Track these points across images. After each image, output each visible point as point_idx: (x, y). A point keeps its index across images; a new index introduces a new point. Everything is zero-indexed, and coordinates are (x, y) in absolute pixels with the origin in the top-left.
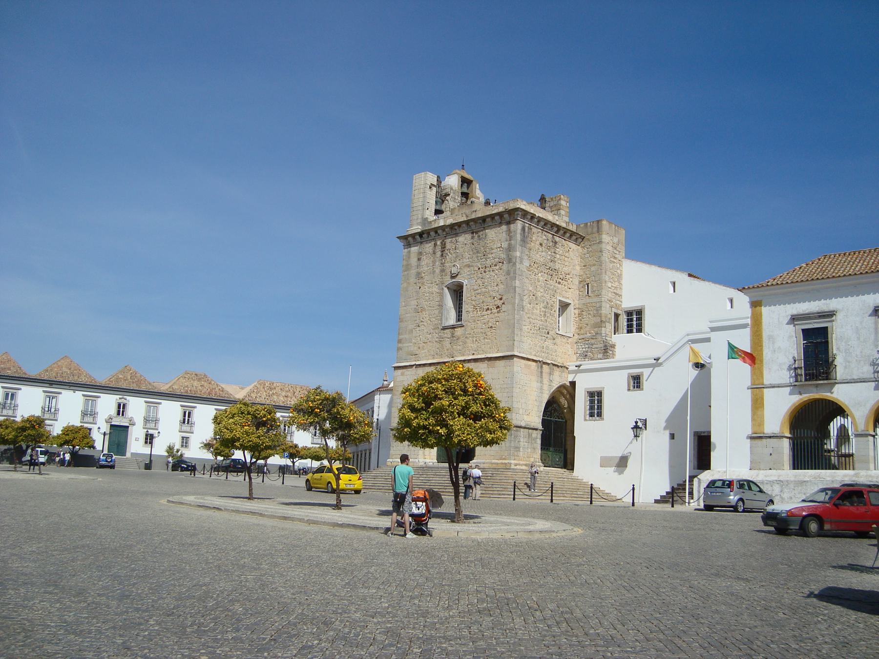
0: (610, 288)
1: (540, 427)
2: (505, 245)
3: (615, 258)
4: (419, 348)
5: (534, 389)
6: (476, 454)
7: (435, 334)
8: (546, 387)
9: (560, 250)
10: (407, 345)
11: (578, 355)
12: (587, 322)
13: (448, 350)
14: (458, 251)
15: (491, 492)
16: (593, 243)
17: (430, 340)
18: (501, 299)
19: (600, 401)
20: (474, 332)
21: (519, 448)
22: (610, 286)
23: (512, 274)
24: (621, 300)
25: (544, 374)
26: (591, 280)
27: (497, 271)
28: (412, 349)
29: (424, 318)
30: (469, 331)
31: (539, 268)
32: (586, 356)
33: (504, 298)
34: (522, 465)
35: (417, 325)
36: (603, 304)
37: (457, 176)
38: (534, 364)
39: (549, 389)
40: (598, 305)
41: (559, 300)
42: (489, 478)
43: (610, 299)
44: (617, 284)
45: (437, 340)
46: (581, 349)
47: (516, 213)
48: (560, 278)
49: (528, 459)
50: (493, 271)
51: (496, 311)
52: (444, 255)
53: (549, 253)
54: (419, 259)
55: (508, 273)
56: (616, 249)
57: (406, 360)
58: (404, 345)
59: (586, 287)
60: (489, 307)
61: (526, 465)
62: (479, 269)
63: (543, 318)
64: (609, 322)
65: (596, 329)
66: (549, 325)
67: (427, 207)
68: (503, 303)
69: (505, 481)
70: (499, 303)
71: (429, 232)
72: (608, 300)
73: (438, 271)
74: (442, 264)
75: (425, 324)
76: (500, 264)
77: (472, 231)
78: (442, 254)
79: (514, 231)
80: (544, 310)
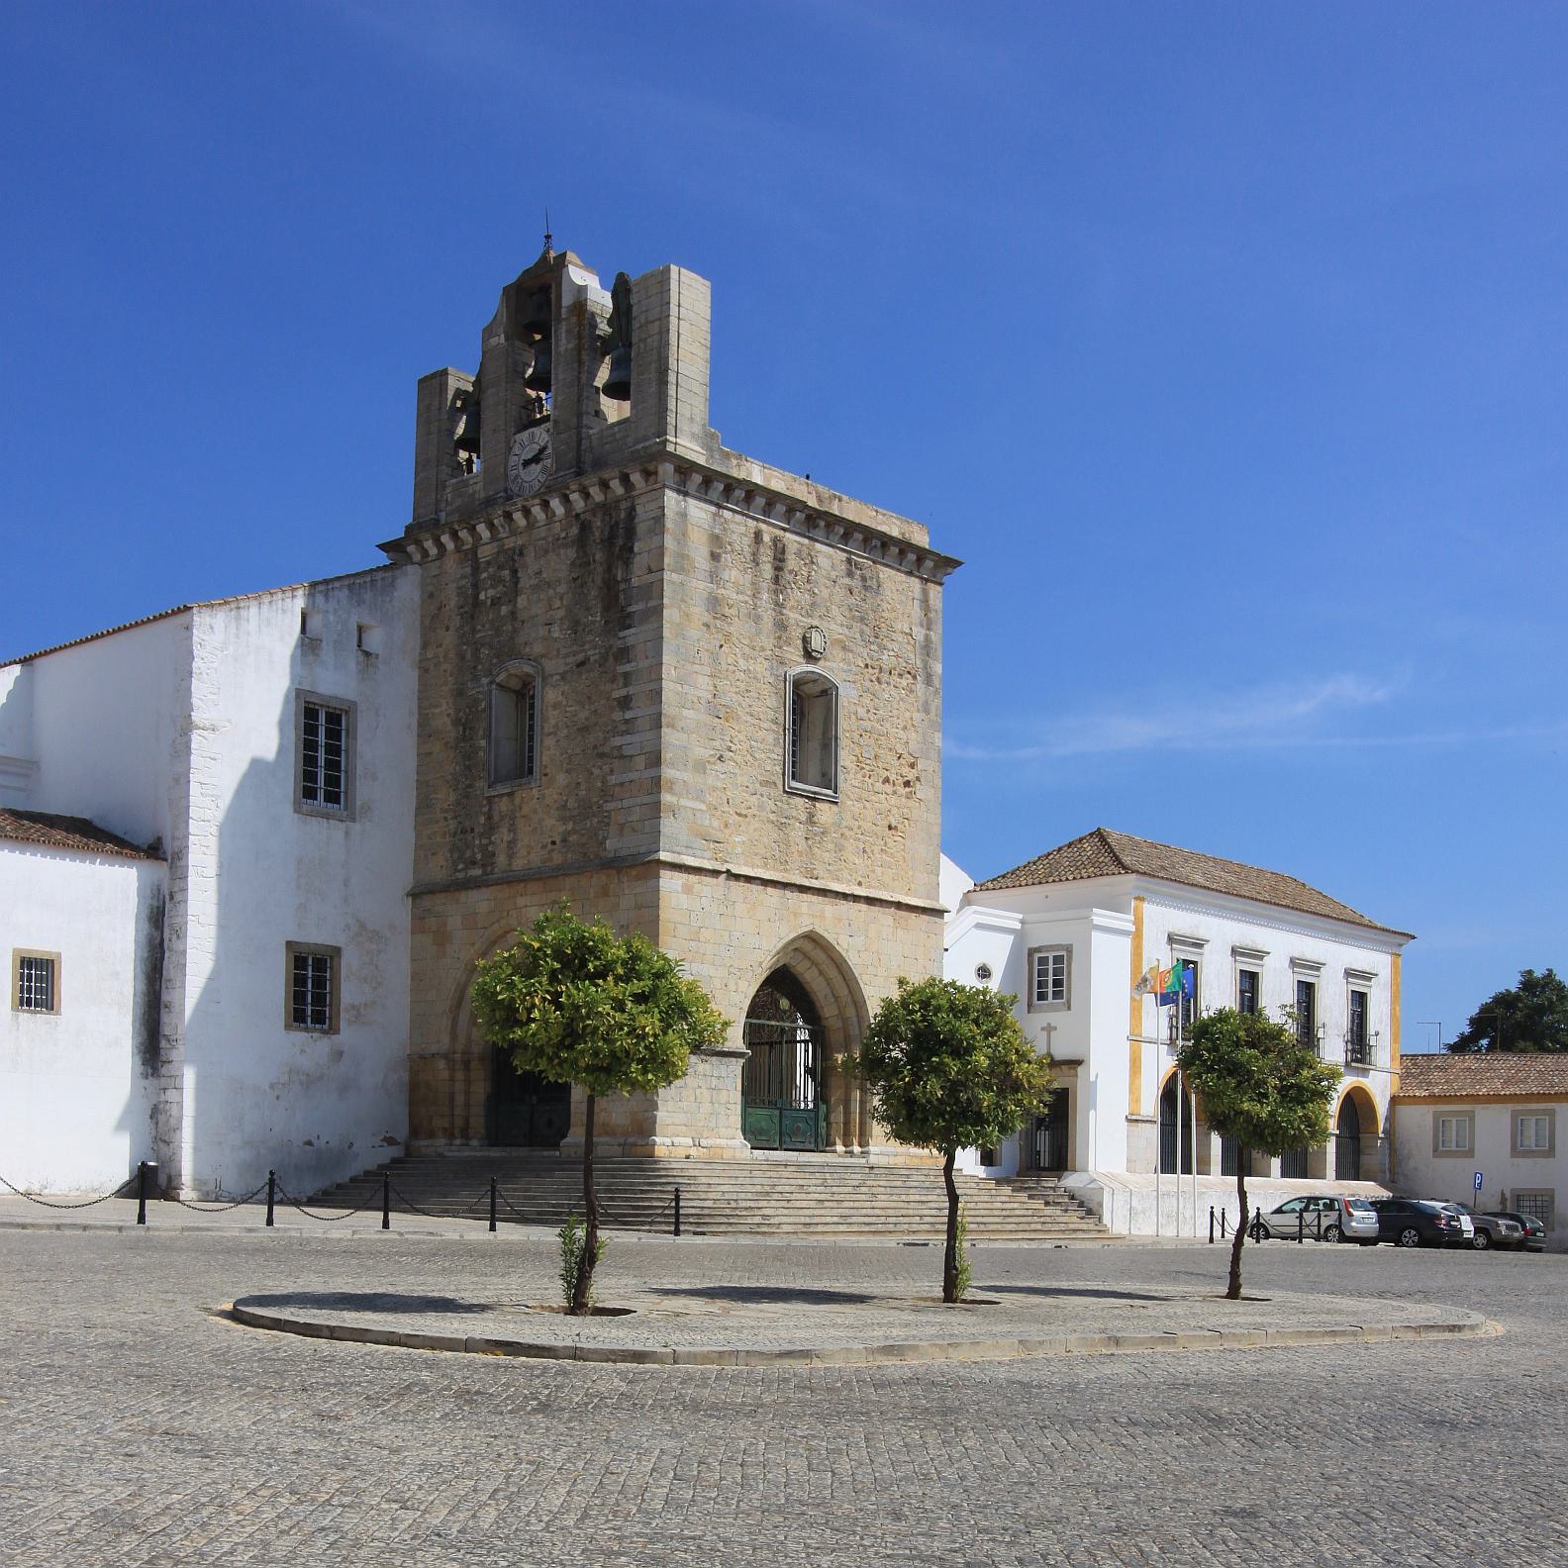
4: (726, 826)
10: (690, 804)
28: (707, 823)
29: (735, 740)
45: (772, 817)
52: (782, 582)
73: (768, 617)
74: (777, 604)
75: (738, 759)
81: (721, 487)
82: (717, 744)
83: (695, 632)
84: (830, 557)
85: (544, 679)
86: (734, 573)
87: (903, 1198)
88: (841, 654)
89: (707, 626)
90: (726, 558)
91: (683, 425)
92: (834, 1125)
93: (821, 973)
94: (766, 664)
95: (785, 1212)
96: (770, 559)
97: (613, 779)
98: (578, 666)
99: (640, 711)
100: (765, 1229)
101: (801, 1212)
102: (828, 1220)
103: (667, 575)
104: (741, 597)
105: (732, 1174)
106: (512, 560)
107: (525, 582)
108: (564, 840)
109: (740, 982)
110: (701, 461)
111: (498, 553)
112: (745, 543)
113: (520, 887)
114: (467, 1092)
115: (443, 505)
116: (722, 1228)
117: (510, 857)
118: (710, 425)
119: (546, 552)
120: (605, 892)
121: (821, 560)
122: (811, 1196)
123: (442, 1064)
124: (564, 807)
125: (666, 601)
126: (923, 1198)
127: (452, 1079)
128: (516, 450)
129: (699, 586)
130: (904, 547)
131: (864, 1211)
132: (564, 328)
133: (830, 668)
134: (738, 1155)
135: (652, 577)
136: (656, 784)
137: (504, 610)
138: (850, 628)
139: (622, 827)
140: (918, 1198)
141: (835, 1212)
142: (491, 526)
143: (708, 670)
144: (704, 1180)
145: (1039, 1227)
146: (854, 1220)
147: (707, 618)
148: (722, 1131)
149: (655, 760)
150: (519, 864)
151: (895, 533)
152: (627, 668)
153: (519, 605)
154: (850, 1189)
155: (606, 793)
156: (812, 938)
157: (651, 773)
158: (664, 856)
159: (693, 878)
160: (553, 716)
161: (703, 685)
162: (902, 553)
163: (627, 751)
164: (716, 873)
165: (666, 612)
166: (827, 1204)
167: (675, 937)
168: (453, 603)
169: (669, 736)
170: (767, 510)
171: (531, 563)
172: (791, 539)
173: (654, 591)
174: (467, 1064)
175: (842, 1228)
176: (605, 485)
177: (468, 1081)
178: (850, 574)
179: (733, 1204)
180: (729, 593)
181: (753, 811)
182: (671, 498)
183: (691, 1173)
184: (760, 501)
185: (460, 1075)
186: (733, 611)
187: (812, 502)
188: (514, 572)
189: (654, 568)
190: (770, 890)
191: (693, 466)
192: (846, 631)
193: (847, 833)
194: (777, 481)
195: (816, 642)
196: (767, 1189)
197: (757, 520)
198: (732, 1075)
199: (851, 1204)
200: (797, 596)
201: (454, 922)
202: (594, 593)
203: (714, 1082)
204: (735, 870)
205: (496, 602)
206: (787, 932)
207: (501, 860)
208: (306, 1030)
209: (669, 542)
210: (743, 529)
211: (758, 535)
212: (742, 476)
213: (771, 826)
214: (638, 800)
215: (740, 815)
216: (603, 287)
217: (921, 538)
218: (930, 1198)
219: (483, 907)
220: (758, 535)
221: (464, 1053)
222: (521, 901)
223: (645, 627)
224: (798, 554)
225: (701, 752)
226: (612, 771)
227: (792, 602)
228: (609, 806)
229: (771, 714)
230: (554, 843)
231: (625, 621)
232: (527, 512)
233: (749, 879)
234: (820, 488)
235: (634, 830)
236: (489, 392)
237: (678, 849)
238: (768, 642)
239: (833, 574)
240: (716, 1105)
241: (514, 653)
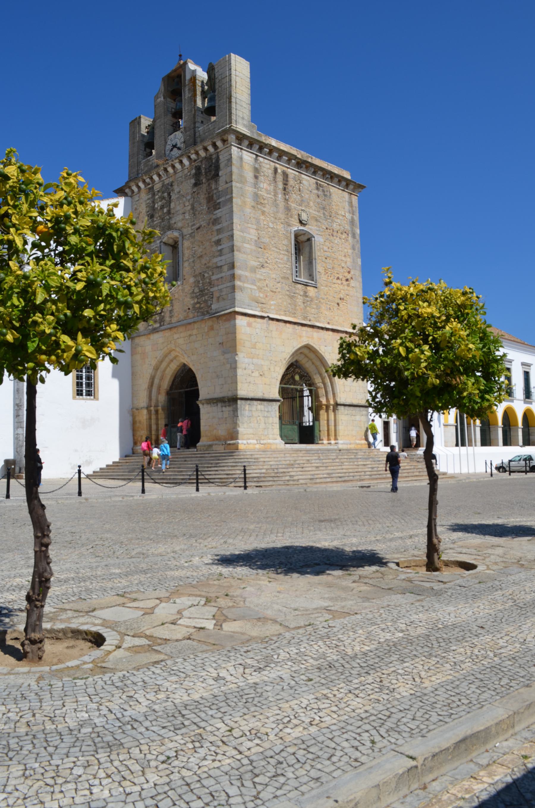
4: (266, 296)
13: (301, 309)
18: (349, 272)
28: (257, 295)
33: (352, 273)
45: (288, 293)
57: (249, 306)
58: (246, 285)
68: (352, 278)
70: (349, 276)
74: (285, 199)
75: (270, 266)
81: (258, 147)
82: (261, 260)
83: (248, 210)
84: (307, 180)
85: (183, 238)
86: (265, 185)
87: (356, 463)
88: (315, 223)
89: (253, 207)
90: (261, 178)
91: (240, 120)
92: (322, 432)
93: (313, 363)
94: (282, 226)
95: (301, 473)
96: (282, 180)
97: (214, 278)
98: (197, 229)
99: (225, 245)
100: (291, 483)
101: (309, 473)
102: (321, 476)
103: (234, 184)
104: (269, 196)
105: (275, 456)
106: (168, 188)
107: (174, 196)
108: (194, 307)
110: (248, 135)
111: (163, 186)
112: (270, 172)
113: (175, 330)
114: (157, 424)
115: (140, 171)
116: (270, 483)
117: (171, 317)
118: (252, 121)
119: (182, 182)
120: (212, 328)
121: (304, 182)
122: (313, 465)
123: (145, 412)
124: (193, 292)
125: (234, 195)
126: (365, 463)
127: (150, 419)
128: (169, 143)
129: (249, 189)
130: (340, 179)
131: (339, 471)
132: (187, 89)
133: (312, 229)
134: (278, 447)
135: (228, 185)
136: (233, 276)
137: (165, 210)
138: (319, 212)
139: (218, 298)
140: (362, 463)
141: (324, 472)
142: (159, 176)
143: (255, 227)
144: (262, 460)
145: (417, 474)
146: (334, 475)
147: (253, 204)
149: (232, 266)
150: (174, 320)
151: (336, 172)
152: (218, 227)
153: (172, 207)
154: (331, 461)
155: (210, 284)
156: (308, 347)
157: (231, 272)
158: (237, 309)
159: (252, 320)
160: (187, 253)
161: (252, 234)
162: (339, 181)
163: (219, 264)
164: (262, 317)
165: (234, 200)
166: (321, 468)
168: (144, 211)
169: (239, 256)
170: (279, 158)
171: (176, 188)
172: (292, 172)
173: (229, 191)
174: (157, 412)
175: (328, 480)
176: (206, 149)
177: (157, 419)
178: (317, 189)
179: (276, 471)
180: (263, 193)
181: (279, 290)
182: (235, 150)
183: (256, 456)
184: (276, 154)
185: (153, 417)
186: (266, 202)
187: (299, 156)
188: (169, 194)
189: (228, 181)
190: (288, 325)
191: (245, 137)
192: (317, 213)
193: (322, 301)
194: (284, 147)
195: (304, 217)
196: (292, 462)
197: (275, 162)
199: (332, 468)
200: (294, 196)
201: (148, 348)
202: (202, 196)
203: (266, 414)
204: (272, 316)
205: (162, 207)
206: (297, 345)
207: (167, 319)
208: (83, 399)
209: (235, 169)
210: (268, 166)
211: (276, 170)
212: (267, 142)
213: (287, 297)
214: (225, 286)
215: (272, 291)
216: (203, 70)
217: (347, 175)
218: (368, 463)
219: (161, 340)
220: (276, 170)
221: (155, 406)
222: (176, 336)
223: (225, 208)
224: (294, 178)
225: (253, 263)
226: (213, 274)
227: (292, 199)
228: (212, 290)
229: (285, 248)
230: (189, 309)
231: (217, 206)
232: (173, 167)
233: (278, 320)
234: (302, 152)
235: (224, 299)
236: (158, 121)
238: (281, 215)
239: (310, 189)
241: (170, 228)
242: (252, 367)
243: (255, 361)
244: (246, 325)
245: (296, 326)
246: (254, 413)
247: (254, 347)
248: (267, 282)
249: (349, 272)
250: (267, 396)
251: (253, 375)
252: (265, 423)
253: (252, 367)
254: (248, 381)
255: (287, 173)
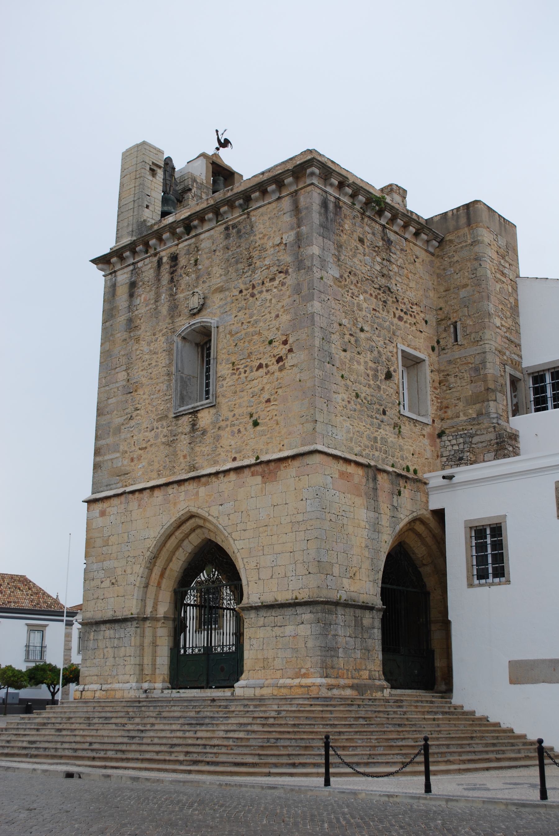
0: (498, 327)
1: (378, 602)
2: (289, 237)
3: (503, 274)
4: (132, 460)
5: (363, 524)
6: (245, 668)
7: (160, 429)
8: (385, 521)
9: (397, 257)
11: (444, 459)
12: (457, 394)
13: (185, 457)
14: (200, 267)
15: (274, 760)
16: (460, 246)
17: (152, 441)
18: (285, 343)
19: (498, 545)
20: (234, 415)
21: (336, 649)
22: (498, 324)
23: (305, 291)
24: (518, 352)
25: (380, 493)
26: (461, 314)
27: (275, 290)
30: (225, 411)
31: (359, 285)
32: (461, 459)
33: (290, 341)
34: (344, 687)
35: (129, 416)
36: (490, 357)
37: (205, 160)
38: (360, 472)
39: (393, 525)
40: (478, 360)
41: (403, 351)
42: (271, 721)
43: (500, 348)
44: (510, 321)
46: (450, 448)
47: (309, 171)
48: (402, 310)
49: (356, 674)
50: (267, 291)
51: (276, 367)
53: (378, 259)
54: (131, 295)
55: (297, 289)
56: (503, 258)
58: (107, 457)
59: (452, 330)
60: (261, 361)
61: (352, 687)
62: (241, 292)
63: (372, 382)
64: (503, 392)
65: (478, 406)
66: (385, 396)
67: (146, 203)
68: (291, 351)
69: (307, 729)
71: (148, 242)
72: (496, 350)
73: (164, 310)
74: (171, 295)
76: (282, 274)
77: (224, 226)
78: (172, 278)
79: (307, 208)
80: (373, 366)
109: (134, 566)
148: (121, 677)
159: (105, 505)
167: (94, 547)
198: (128, 635)
237: (102, 489)
240: (117, 659)
242: (101, 574)
243: (107, 564)
244: (98, 515)
245: (170, 490)
246: (100, 644)
247: (106, 544)
248: (135, 438)
249: (285, 343)
250: (119, 615)
251: (103, 585)
252: (114, 657)
253: (101, 574)
254: (95, 596)
255: (178, 252)
